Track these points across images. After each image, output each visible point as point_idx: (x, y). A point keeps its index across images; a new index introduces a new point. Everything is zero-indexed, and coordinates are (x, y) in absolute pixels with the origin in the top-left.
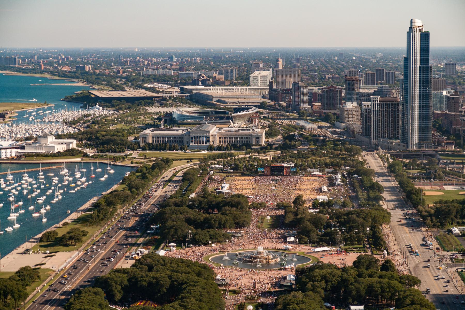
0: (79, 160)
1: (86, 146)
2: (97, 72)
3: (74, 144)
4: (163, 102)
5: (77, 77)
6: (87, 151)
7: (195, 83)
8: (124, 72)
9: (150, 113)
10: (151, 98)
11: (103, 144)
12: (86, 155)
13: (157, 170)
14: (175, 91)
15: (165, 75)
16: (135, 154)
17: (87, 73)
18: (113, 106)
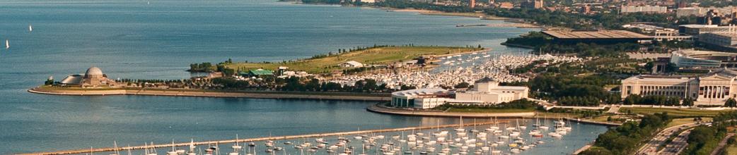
0: (531, 114)
1: (541, 96)
2: (552, 9)
3: (524, 93)
4: (653, 46)
5: (523, 17)
6: (542, 102)
7: (702, 20)
8: (591, 10)
9: (634, 60)
10: (635, 40)
11: (566, 95)
12: (541, 109)
13: (648, 127)
14: (671, 34)
15: (655, 14)
16: (614, 108)
17: (537, 11)
18: (577, 50)
